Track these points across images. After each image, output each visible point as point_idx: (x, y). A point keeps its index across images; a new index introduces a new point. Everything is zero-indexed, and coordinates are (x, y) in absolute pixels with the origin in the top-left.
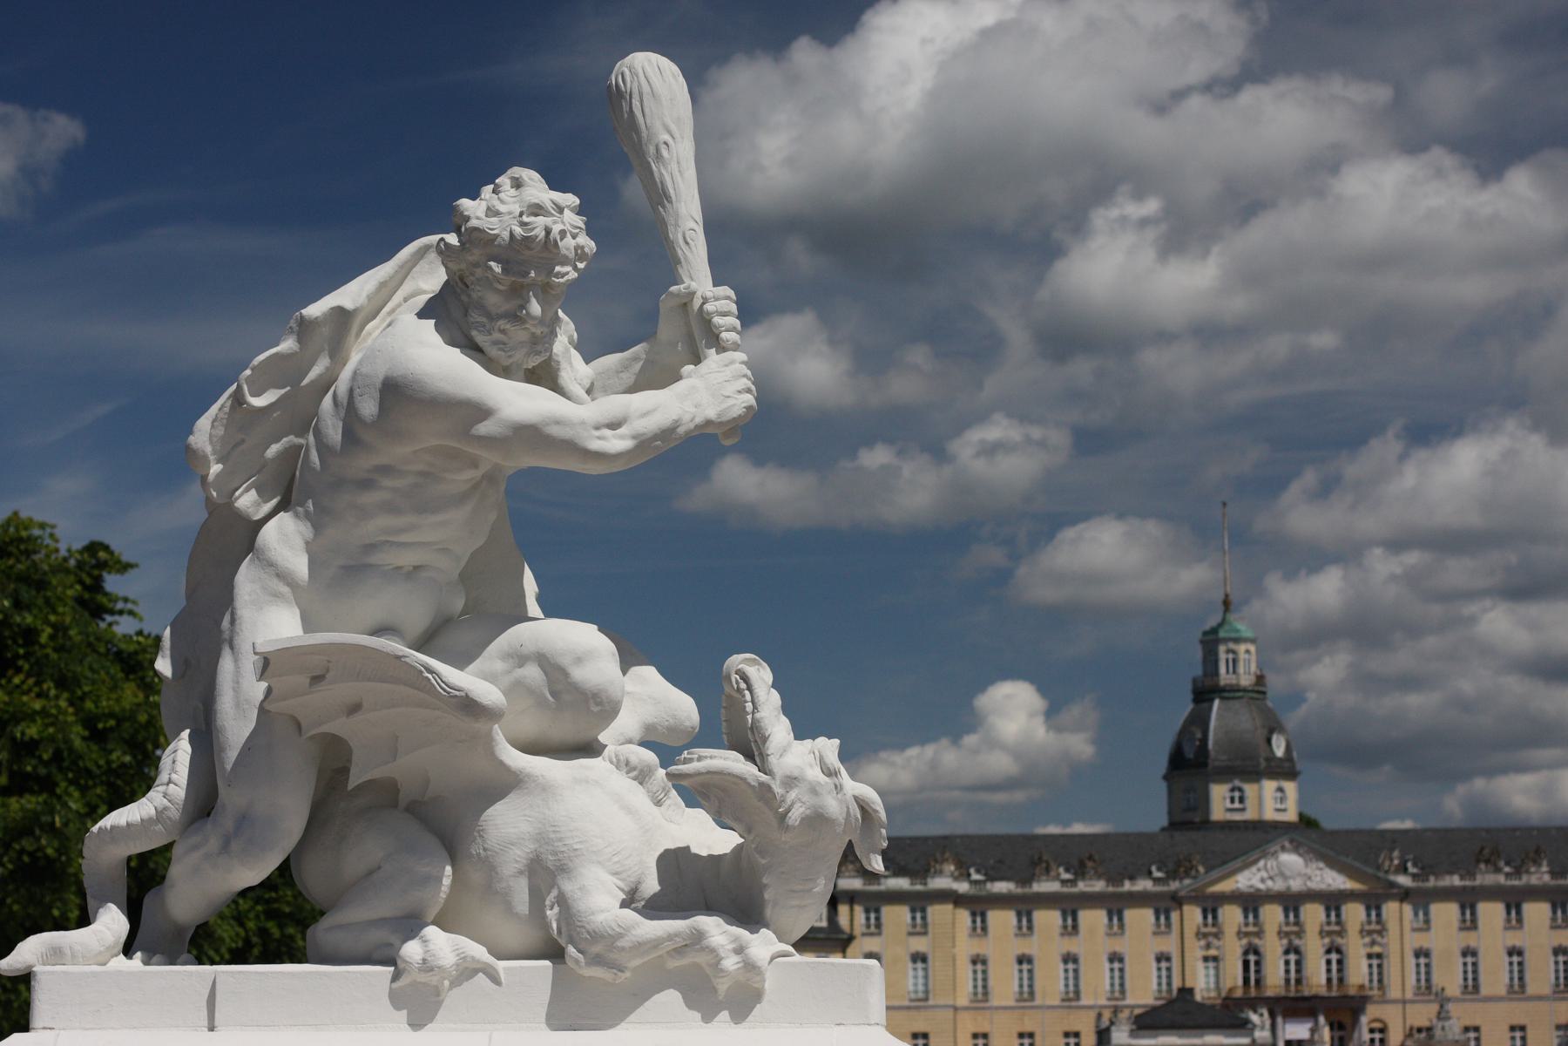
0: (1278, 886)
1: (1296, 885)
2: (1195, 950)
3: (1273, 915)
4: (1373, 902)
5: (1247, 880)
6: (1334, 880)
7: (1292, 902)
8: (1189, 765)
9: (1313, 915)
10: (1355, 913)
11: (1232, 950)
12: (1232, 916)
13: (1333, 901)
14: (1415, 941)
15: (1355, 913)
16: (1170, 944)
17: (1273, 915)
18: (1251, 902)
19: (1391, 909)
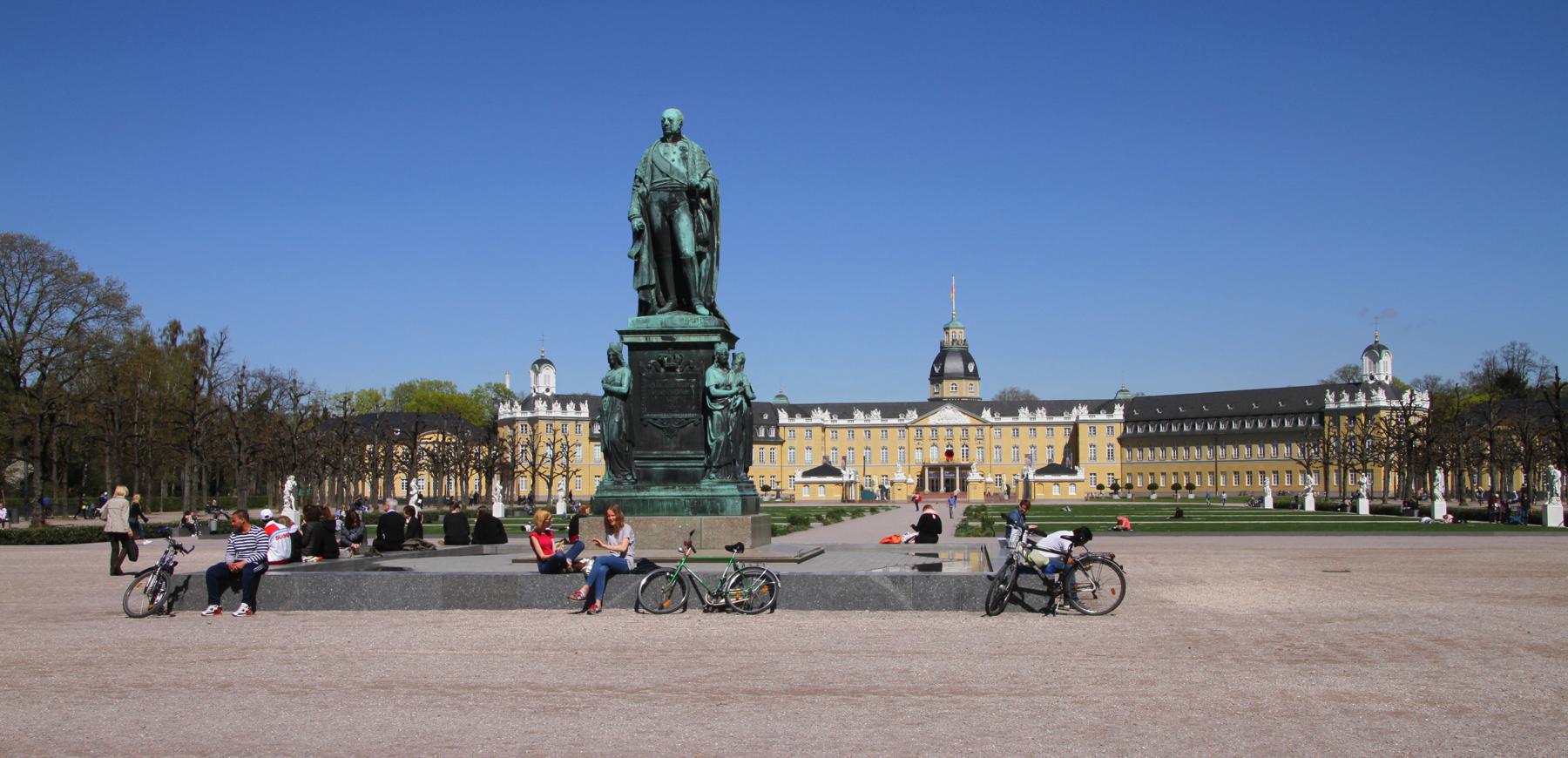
0: (945, 422)
1: (951, 422)
2: (914, 444)
3: (943, 432)
4: (979, 427)
5: (933, 419)
6: (966, 420)
7: (950, 427)
8: (937, 378)
9: (958, 432)
10: (973, 432)
12: (927, 432)
13: (965, 427)
14: (995, 443)
15: (973, 432)
16: (905, 444)
17: (943, 432)
18: (935, 427)
19: (986, 429)
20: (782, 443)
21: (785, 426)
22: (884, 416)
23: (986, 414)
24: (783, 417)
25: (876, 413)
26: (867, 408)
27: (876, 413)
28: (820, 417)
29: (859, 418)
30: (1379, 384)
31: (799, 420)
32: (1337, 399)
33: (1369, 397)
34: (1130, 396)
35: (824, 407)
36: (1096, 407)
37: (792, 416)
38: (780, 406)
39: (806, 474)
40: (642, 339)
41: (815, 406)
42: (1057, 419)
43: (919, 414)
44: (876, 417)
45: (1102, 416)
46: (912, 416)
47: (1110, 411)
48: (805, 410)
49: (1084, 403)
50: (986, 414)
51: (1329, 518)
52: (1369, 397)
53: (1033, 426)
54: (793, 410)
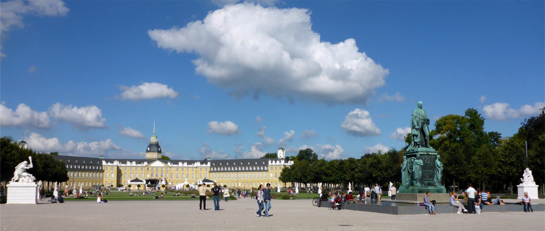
4: (167, 168)
7: (157, 168)
10: (164, 169)
11: (150, 172)
13: (162, 167)
17: (155, 169)
18: (153, 167)
20: (104, 171)
21: (105, 166)
22: (137, 163)
23: (169, 164)
24: (104, 163)
25: (134, 163)
26: (131, 161)
27: (134, 163)
28: (116, 163)
29: (129, 164)
30: (282, 159)
31: (109, 164)
32: (272, 162)
33: (280, 162)
34: (211, 160)
35: (118, 160)
36: (202, 163)
37: (107, 162)
38: (103, 159)
39: (131, 181)
40: (423, 153)
41: (115, 160)
42: (190, 166)
43: (148, 163)
44: (134, 163)
45: (204, 165)
46: (146, 164)
47: (207, 164)
48: (112, 161)
49: (199, 161)
50: (169, 164)
51: (303, 195)
52: (280, 162)
53: (183, 168)
54: (107, 161)
